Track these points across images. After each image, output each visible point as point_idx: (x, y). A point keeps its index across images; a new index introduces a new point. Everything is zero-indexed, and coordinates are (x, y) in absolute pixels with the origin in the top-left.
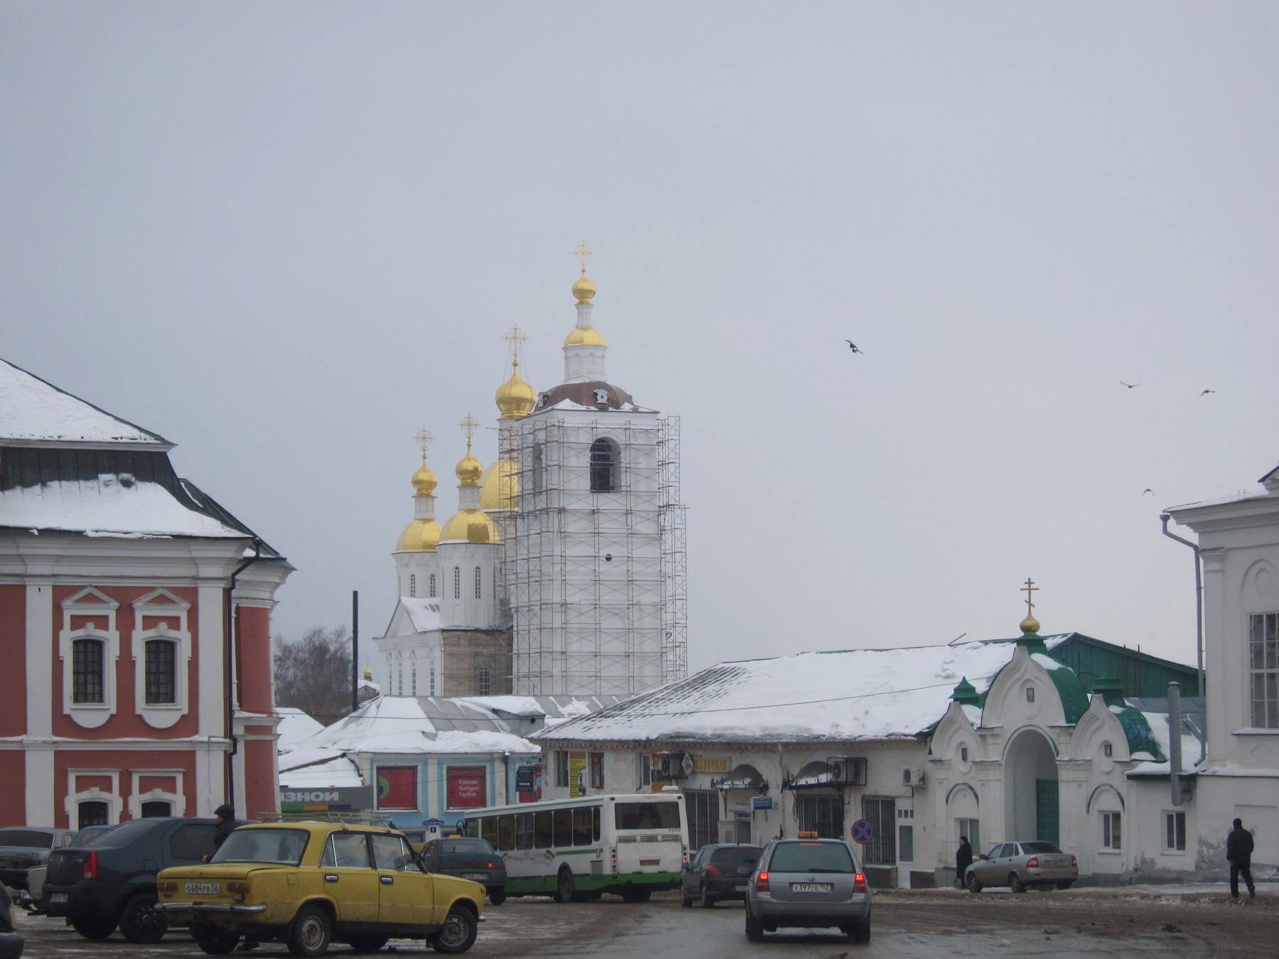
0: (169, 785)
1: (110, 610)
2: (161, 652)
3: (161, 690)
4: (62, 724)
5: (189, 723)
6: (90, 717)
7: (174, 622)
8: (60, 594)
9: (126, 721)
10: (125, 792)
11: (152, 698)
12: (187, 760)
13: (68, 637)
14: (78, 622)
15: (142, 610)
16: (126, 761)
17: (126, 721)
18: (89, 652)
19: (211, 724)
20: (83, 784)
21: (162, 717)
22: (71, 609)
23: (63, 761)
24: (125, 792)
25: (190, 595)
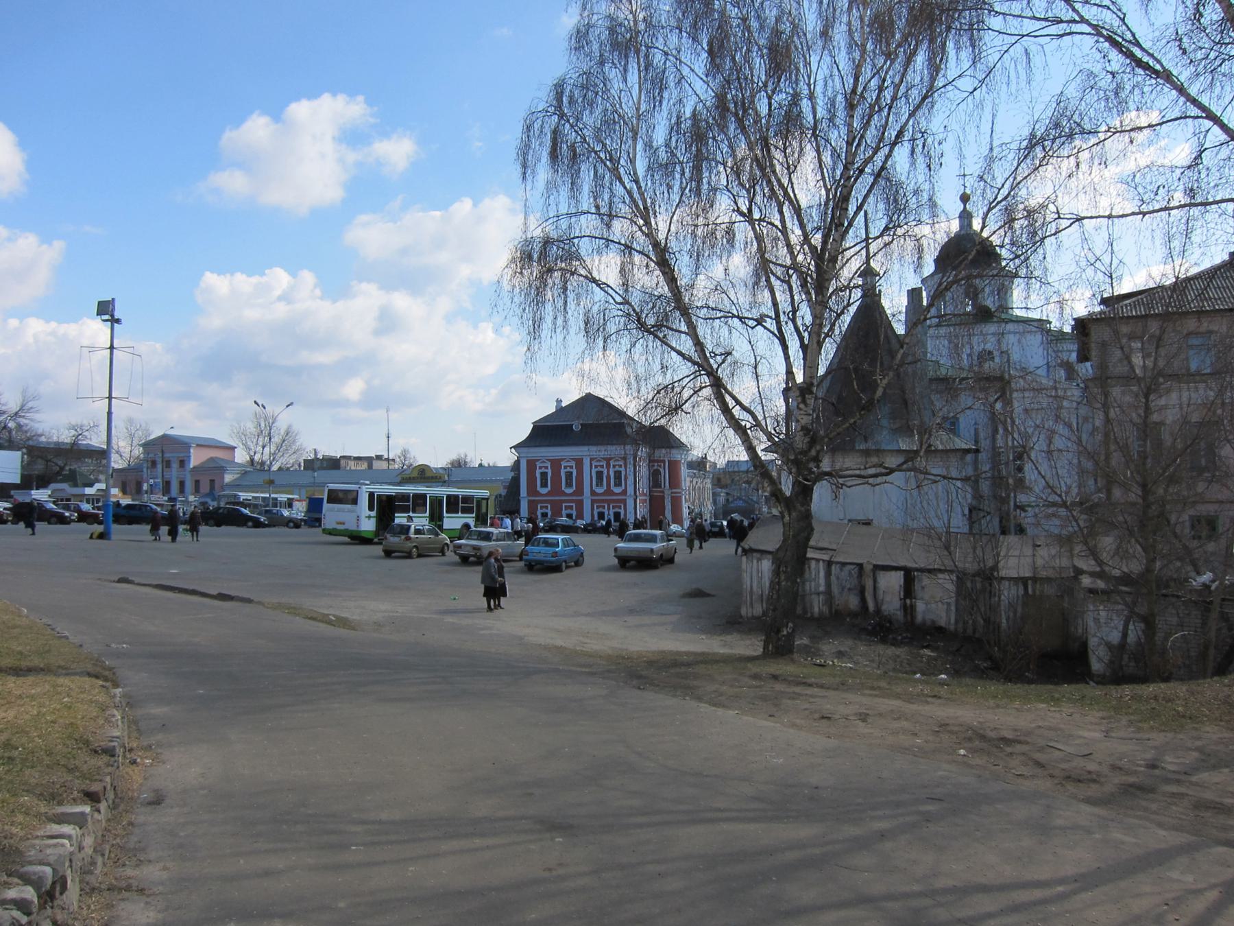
0: (620, 507)
1: (604, 463)
2: (618, 475)
3: (618, 484)
4: (593, 493)
5: (625, 492)
6: (600, 490)
7: (620, 466)
8: (591, 460)
9: (609, 491)
10: (609, 509)
11: (597, 485)
12: (624, 502)
13: (594, 471)
14: (596, 467)
15: (612, 463)
16: (609, 502)
17: (609, 491)
18: (599, 475)
19: (630, 490)
20: (598, 507)
21: (617, 490)
22: (594, 463)
23: (593, 502)
24: (609, 509)
25: (625, 459)
